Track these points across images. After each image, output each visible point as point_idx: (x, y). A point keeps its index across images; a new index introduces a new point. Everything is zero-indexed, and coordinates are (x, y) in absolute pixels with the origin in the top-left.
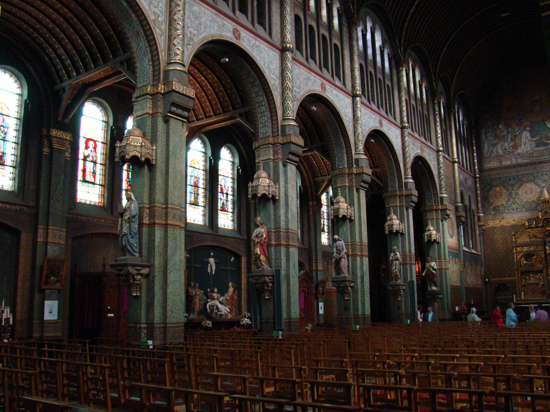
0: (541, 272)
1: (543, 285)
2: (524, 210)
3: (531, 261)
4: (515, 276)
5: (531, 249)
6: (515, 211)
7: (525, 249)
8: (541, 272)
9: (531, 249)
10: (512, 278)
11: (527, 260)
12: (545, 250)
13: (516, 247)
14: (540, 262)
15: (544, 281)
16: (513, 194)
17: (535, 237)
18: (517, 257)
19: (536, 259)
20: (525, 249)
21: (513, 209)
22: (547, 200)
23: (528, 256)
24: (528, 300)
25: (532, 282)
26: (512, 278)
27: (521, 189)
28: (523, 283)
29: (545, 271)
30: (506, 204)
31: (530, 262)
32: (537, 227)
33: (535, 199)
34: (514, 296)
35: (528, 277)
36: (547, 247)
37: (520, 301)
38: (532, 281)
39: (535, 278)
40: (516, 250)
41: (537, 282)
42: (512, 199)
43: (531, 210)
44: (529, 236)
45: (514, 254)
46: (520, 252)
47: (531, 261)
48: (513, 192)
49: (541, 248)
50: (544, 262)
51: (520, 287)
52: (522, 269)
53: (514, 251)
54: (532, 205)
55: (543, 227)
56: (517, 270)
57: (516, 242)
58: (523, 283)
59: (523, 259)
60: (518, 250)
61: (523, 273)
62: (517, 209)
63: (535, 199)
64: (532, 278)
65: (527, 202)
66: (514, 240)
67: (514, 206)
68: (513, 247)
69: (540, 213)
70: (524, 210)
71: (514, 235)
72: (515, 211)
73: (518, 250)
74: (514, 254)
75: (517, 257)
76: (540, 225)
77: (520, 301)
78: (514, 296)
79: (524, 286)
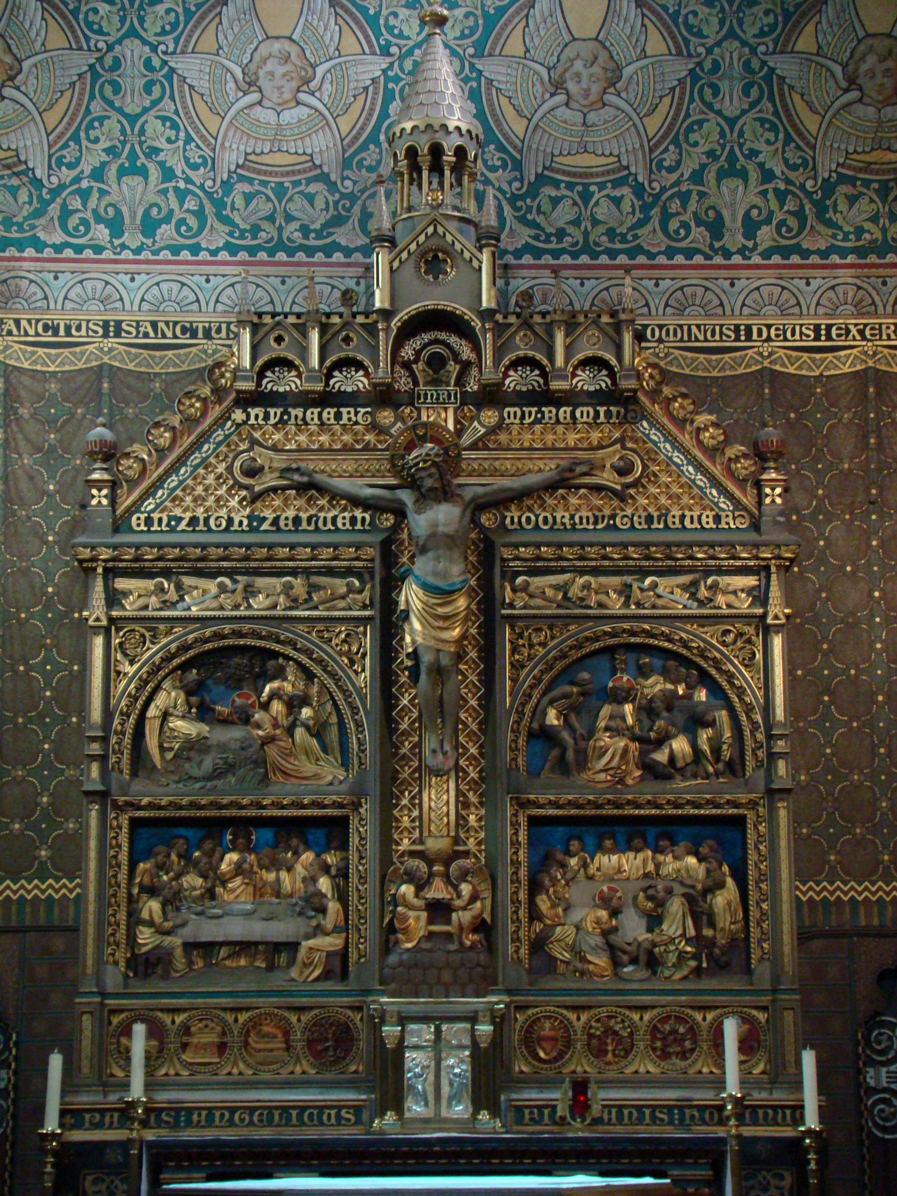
0: (333, 830)
1: (338, 966)
2: (216, 236)
3: (245, 719)
4: (72, 868)
5: (259, 603)
6: (133, 238)
7: (202, 598)
8: (333, 830)
9: (259, 603)
10: (31, 889)
11: (204, 713)
12: (390, 622)
13: (111, 573)
14: (330, 736)
15: (343, 928)
16: (132, 78)
17: (309, 488)
18: (110, 673)
19: (294, 704)
20: (202, 598)
21: (116, 226)
22: (450, 144)
23: (222, 667)
24: (181, 1114)
25: (236, 929)
26: (31, 889)
27: (208, 42)
28: (146, 937)
29: (363, 828)
30: (56, 162)
31: (234, 734)
32: (325, 399)
33: (323, 145)
34: (56, 1062)
35: (193, 881)
36: (411, 596)
37: (100, 1116)
38: (237, 915)
39: (259, 891)
40: (113, 598)
41: (280, 930)
42: (113, 125)
43: (281, 246)
44: (252, 472)
45: (83, 630)
46: (151, 625)
47: (245, 719)
48: (133, 51)
49: (351, 599)
50: (365, 737)
51: (113, 978)
52: (151, 794)
53: (96, 611)
54: (297, 207)
55: (383, 397)
56: (102, 796)
57: (120, 525)
58: (146, 937)
59: (169, 696)
60: (130, 607)
61: (153, 831)
62: (149, 227)
63: (323, 145)
64: (237, 893)
65: (247, 168)
66: (100, 498)
67: (132, 194)
68: (86, 569)
69: (381, 259)
70: (216, 236)
71: (109, 454)
72: (133, 238)
73: (130, 607)
74: (83, 630)
75: (108, 675)
76: (358, 382)
77: (100, 1116)
78: (56, 1062)
79: (147, 965)
